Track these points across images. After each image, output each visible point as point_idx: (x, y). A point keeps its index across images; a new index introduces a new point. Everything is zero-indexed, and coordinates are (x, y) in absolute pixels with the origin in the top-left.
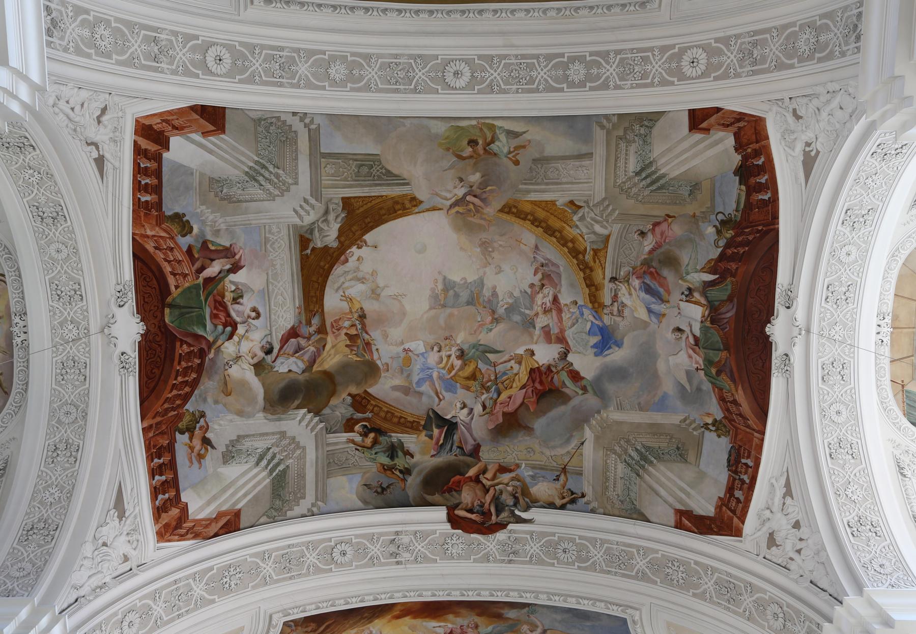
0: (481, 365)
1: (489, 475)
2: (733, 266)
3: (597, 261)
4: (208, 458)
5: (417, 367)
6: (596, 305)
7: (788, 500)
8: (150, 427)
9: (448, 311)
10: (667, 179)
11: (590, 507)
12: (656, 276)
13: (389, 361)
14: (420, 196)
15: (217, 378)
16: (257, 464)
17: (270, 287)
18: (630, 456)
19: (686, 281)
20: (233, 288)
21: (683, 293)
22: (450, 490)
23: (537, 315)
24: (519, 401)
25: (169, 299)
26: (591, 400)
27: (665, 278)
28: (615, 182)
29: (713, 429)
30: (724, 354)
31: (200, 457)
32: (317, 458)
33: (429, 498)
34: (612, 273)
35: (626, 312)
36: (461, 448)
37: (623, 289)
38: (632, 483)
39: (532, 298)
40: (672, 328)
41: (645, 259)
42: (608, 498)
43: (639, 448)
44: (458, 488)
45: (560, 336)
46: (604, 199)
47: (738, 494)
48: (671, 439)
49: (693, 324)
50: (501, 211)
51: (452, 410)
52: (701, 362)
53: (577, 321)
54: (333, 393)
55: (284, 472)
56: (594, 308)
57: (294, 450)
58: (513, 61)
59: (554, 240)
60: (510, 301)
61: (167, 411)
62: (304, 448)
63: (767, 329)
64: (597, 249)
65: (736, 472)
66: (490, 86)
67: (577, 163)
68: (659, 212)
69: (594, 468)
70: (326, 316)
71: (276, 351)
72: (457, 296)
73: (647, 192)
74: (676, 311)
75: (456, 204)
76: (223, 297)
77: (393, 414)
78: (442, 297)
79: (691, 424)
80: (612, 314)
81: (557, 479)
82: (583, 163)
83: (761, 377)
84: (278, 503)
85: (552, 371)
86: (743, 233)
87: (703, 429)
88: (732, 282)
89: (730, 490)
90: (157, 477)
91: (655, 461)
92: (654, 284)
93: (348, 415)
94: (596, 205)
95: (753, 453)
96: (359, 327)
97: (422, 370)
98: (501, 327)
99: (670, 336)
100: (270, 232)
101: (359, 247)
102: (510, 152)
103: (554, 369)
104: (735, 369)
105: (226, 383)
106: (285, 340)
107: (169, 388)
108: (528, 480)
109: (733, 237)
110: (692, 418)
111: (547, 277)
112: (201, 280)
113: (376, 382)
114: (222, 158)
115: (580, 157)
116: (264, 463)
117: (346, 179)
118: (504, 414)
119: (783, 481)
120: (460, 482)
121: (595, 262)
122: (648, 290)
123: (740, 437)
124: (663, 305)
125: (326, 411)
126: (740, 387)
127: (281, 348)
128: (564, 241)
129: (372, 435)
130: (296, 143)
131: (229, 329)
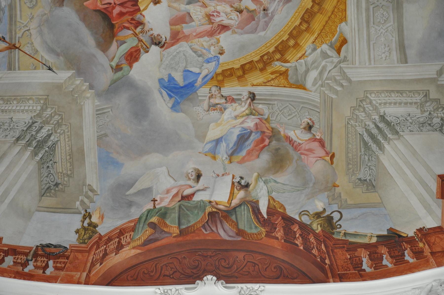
2: (280, 234)
3: (273, 76)
6: (220, 78)
10: (379, 152)
18: (42, 128)
19: (257, 180)
21: (242, 178)
23: (205, 5)
27: (258, 157)
28: (371, 92)
29: (86, 224)
34: (260, 95)
35: (214, 114)
37: (243, 108)
38: (7, 132)
40: (200, 168)
41: (279, 132)
43: (52, 138)
45: (180, 36)
46: (349, 81)
47: (9, 260)
48: (68, 175)
49: (207, 193)
52: (164, 204)
53: (200, 56)
56: (217, 75)
59: (297, 23)
63: (210, 277)
64: (287, 76)
65: (36, 255)
67: (394, 45)
73: (360, 130)
74: (221, 172)
79: (88, 197)
80: (211, 97)
82: (394, 53)
83: (152, 274)
85: (136, 27)
86: (319, 242)
87: (83, 212)
88: (260, 234)
91: (38, 158)
95: (62, 273)
99: (190, 167)
103: (139, 30)
104: (158, 244)
109: (313, 231)
110: (95, 198)
111: (252, 15)
121: (272, 73)
123: (79, 256)
124: (225, 156)
126: (138, 251)
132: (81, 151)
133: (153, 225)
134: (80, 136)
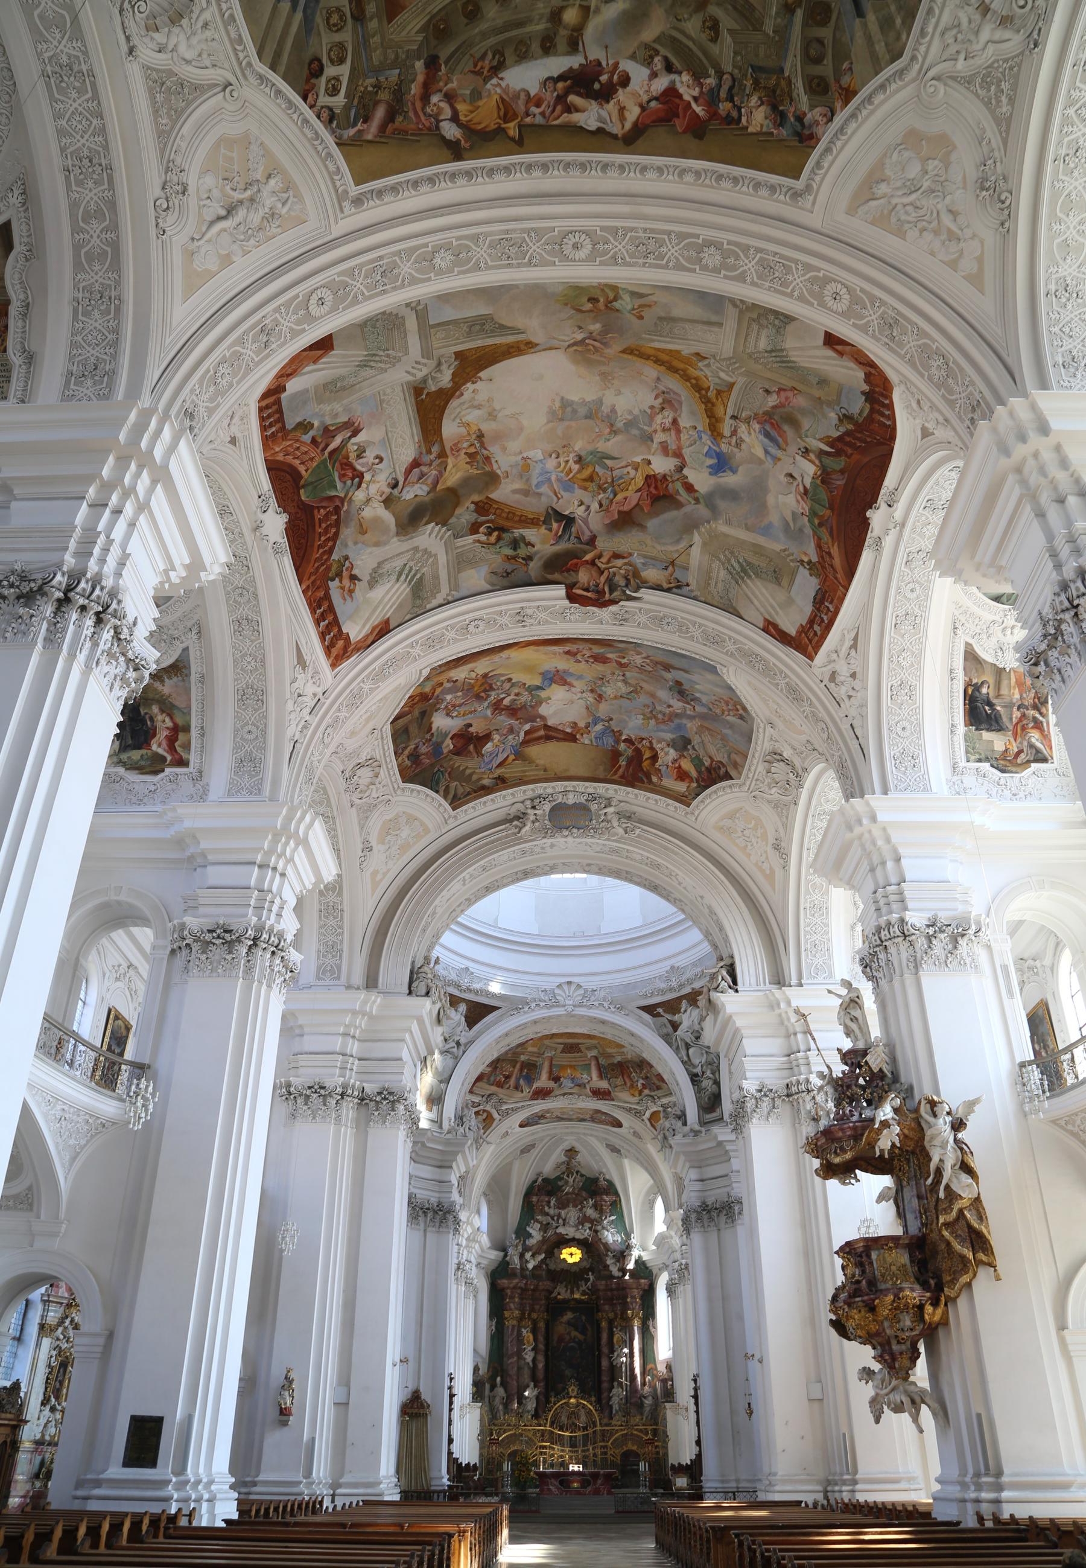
1: (604, 560)
2: (850, 451)
5: (536, 471)
7: (853, 651)
8: (308, 587)
9: (566, 423)
11: (693, 594)
12: (776, 427)
13: (509, 470)
14: (535, 340)
15: (353, 524)
16: (398, 580)
17: (390, 435)
20: (356, 447)
22: (568, 571)
23: (655, 431)
24: (634, 502)
25: (302, 482)
26: (702, 510)
30: (829, 512)
31: (351, 592)
32: (448, 560)
35: (744, 446)
37: (743, 429)
39: (652, 418)
40: (785, 472)
42: (710, 592)
44: (575, 569)
46: (730, 359)
49: (805, 476)
50: (623, 352)
51: (571, 503)
54: (457, 504)
55: (421, 578)
57: (428, 559)
58: (641, 234)
60: (630, 417)
61: (318, 568)
62: (436, 555)
65: (818, 610)
66: (614, 257)
68: (788, 383)
70: (445, 442)
71: (401, 484)
72: (574, 411)
75: (575, 344)
76: (348, 458)
77: (514, 514)
79: (789, 555)
81: (666, 568)
84: (418, 602)
89: (811, 622)
90: (322, 624)
92: (773, 433)
93: (473, 520)
94: (724, 359)
96: (478, 445)
97: (541, 474)
99: (784, 480)
100: (384, 394)
101: (473, 383)
102: (634, 309)
104: (835, 528)
105: (361, 525)
106: (408, 472)
107: (315, 549)
108: (639, 566)
113: (497, 488)
114: (333, 368)
116: (403, 577)
117: (458, 339)
118: (619, 512)
119: (853, 635)
120: (576, 564)
122: (767, 435)
123: (828, 583)
125: (453, 520)
127: (406, 479)
128: (686, 377)
129: (496, 534)
130: (404, 325)
131: (357, 480)
132: (754, 545)
133: (820, 525)
134: (744, 542)
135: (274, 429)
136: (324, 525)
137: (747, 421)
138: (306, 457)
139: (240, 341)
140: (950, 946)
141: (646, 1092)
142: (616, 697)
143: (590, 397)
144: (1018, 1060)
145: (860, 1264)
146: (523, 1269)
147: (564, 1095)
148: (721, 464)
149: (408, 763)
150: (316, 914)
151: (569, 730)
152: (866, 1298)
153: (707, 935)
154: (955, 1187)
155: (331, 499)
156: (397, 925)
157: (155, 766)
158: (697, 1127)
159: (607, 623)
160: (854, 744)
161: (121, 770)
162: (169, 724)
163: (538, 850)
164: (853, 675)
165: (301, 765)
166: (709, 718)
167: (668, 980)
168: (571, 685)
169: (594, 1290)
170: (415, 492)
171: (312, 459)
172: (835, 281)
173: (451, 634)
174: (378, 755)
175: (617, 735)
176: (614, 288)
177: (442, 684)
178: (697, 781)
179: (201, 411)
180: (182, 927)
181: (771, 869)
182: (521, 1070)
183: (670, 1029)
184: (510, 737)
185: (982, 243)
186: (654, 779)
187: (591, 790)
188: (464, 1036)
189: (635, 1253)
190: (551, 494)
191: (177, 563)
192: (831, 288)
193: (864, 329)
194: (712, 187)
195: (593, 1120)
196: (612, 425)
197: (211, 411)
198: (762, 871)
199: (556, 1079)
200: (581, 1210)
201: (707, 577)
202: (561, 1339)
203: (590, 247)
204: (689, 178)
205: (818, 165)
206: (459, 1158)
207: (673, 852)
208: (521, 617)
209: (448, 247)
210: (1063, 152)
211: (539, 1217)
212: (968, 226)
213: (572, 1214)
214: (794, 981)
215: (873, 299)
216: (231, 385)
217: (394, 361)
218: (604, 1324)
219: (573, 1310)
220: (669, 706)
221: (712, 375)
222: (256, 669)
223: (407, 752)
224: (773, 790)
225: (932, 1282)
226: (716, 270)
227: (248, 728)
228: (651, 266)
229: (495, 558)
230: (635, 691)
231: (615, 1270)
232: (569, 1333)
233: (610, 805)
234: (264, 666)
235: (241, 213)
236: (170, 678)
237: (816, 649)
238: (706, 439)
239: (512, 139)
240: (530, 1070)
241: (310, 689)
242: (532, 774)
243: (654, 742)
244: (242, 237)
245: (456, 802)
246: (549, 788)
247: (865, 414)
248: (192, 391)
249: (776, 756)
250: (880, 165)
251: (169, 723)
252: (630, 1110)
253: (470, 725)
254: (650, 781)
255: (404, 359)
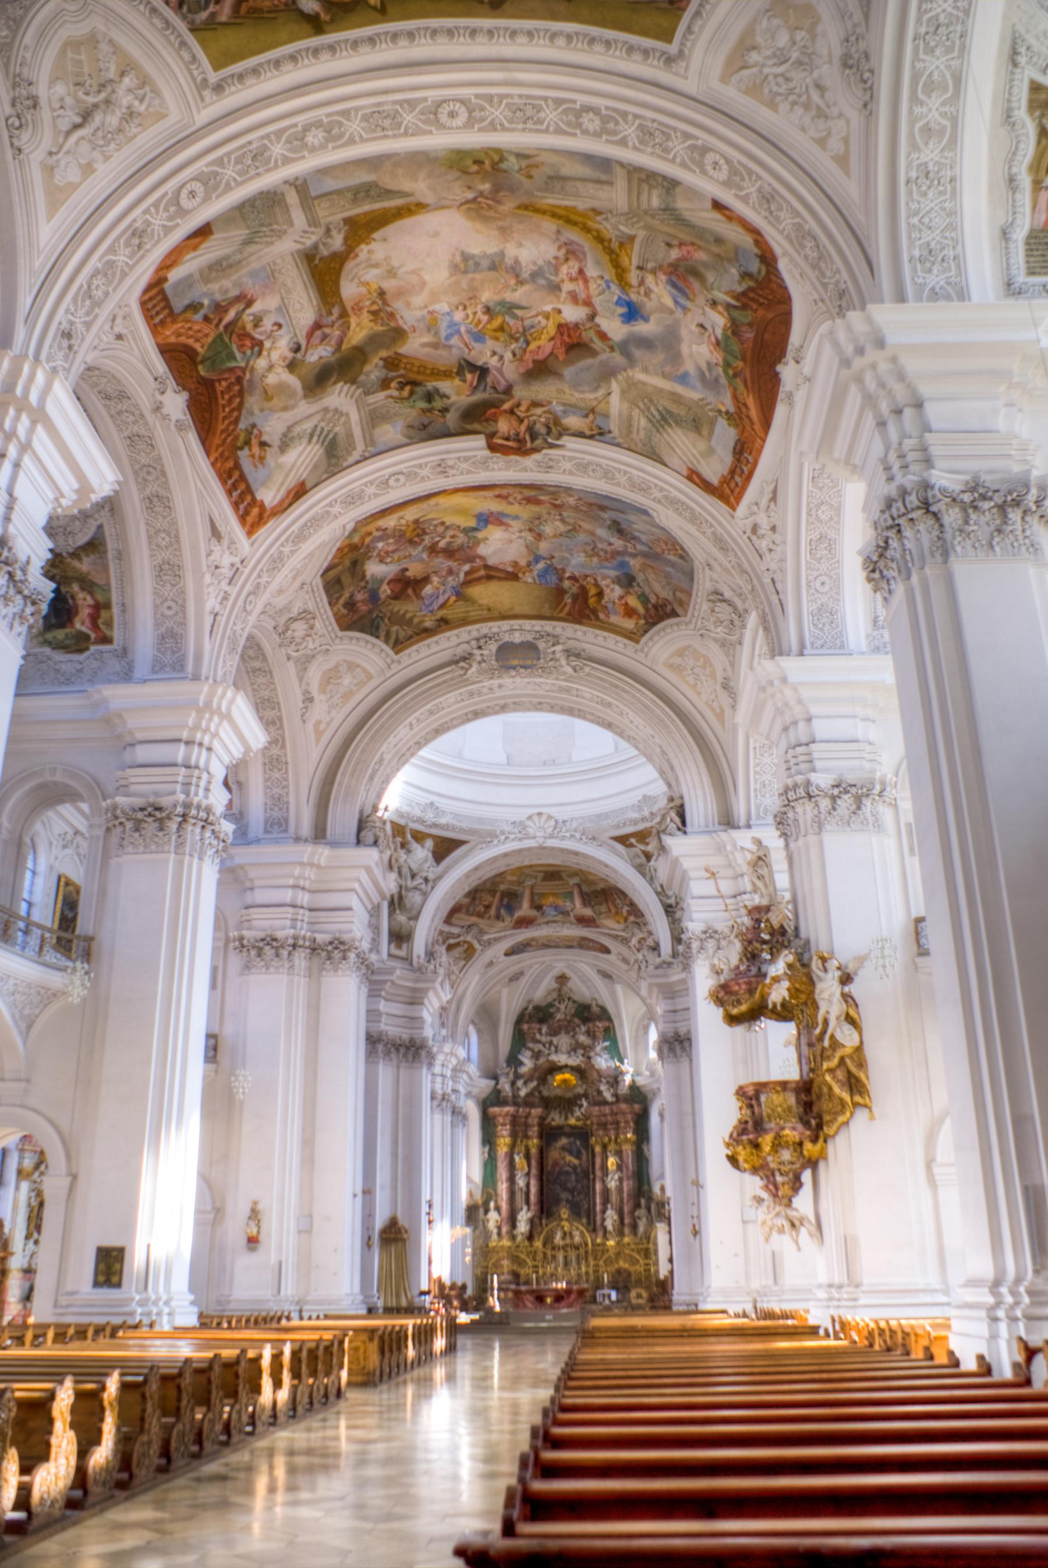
0: (508, 318)
1: (523, 408)
2: (755, 306)
4: (268, 456)
7: (772, 505)
8: (217, 459)
9: (470, 276)
15: (257, 392)
16: (310, 442)
22: (487, 420)
23: (563, 281)
24: (548, 351)
25: (199, 358)
26: (618, 358)
30: (740, 364)
31: (262, 459)
33: (469, 427)
35: (653, 296)
36: (494, 388)
37: (650, 280)
39: (557, 270)
46: (627, 214)
50: (519, 207)
51: (484, 354)
54: (365, 361)
55: (334, 438)
58: (516, 100)
60: (534, 268)
61: (224, 440)
62: (347, 414)
65: (738, 460)
66: (492, 123)
69: (620, 415)
71: (303, 347)
72: (477, 264)
74: (700, 311)
75: (467, 202)
76: (244, 328)
78: (462, 266)
84: (333, 461)
89: (732, 472)
92: (680, 284)
93: (383, 376)
97: (449, 327)
98: (526, 288)
99: (694, 327)
105: (266, 392)
106: (310, 335)
108: (560, 414)
112: (221, 328)
115: (599, 182)
116: (315, 438)
118: (535, 362)
120: (495, 414)
122: (674, 285)
125: (362, 378)
127: (308, 342)
128: (587, 230)
129: (408, 388)
131: (256, 349)
132: (673, 394)
133: (735, 375)
134: (661, 390)
135: (161, 316)
136: (227, 397)
137: (653, 272)
138: (200, 335)
139: (112, 250)
140: (854, 807)
141: (632, 918)
142: (555, 536)
143: (492, 248)
144: (914, 915)
145: (751, 1106)
146: (515, 1096)
147: (547, 923)
148: (632, 313)
149: (344, 611)
150: (260, 768)
151: (510, 569)
152: (751, 1136)
153: (662, 773)
154: (839, 1036)
155: (231, 370)
156: (344, 774)
157: (79, 644)
158: (671, 960)
159: (532, 471)
160: (774, 599)
161: (47, 650)
162: (90, 601)
163: (485, 690)
164: (773, 529)
165: (223, 637)
166: (651, 556)
167: (640, 809)
168: (507, 525)
169: (587, 1117)
170: (319, 354)
171: (206, 335)
172: (713, 150)
173: (371, 490)
174: (311, 607)
175: (560, 573)
176: (498, 151)
177: (370, 534)
178: (645, 618)
179: (80, 328)
180: (115, 807)
181: (721, 708)
182: (501, 899)
183: (643, 859)
184: (450, 579)
185: (848, 121)
186: (602, 616)
187: (538, 628)
188: (431, 870)
189: (628, 1079)
190: (462, 346)
191: (65, 489)
192: (710, 158)
193: (745, 199)
194: (584, 51)
195: (581, 946)
196: (517, 276)
197: (88, 325)
198: (713, 710)
199: (539, 908)
200: (573, 1036)
201: (628, 425)
202: (556, 1164)
203: (466, 115)
204: (561, 42)
205: (689, 30)
206: (431, 994)
207: (624, 690)
208: (442, 468)
209: (318, 124)
210: (923, 30)
211: (530, 1045)
212: (835, 104)
213: (563, 1041)
214: (742, 822)
215: (750, 172)
216: (106, 294)
217: (281, 234)
218: (598, 1149)
219: (568, 1135)
220: (610, 544)
221: (609, 229)
222: (171, 544)
223: (342, 601)
224: (719, 629)
225: (813, 1122)
226: (597, 135)
227: (166, 604)
228: (531, 130)
229: (412, 412)
230: (574, 530)
231: (608, 1096)
232: (564, 1158)
233: (558, 643)
234: (178, 541)
235: (98, 118)
236: (87, 556)
237: (738, 499)
238: (615, 289)
239: (374, 8)
240: (510, 899)
241: (227, 560)
242: (475, 614)
243: (599, 578)
244: (101, 142)
245: (398, 645)
246: (494, 627)
247: (764, 272)
248: (67, 311)
249: (717, 596)
250: (750, 30)
251: (90, 601)
252: (616, 937)
253: (406, 570)
254: (598, 618)
255: (290, 231)
